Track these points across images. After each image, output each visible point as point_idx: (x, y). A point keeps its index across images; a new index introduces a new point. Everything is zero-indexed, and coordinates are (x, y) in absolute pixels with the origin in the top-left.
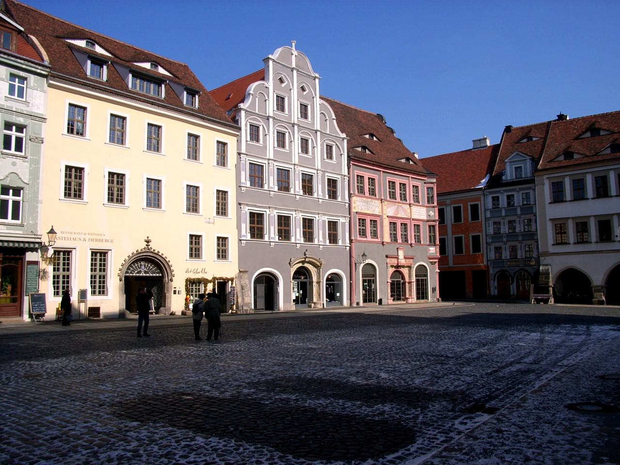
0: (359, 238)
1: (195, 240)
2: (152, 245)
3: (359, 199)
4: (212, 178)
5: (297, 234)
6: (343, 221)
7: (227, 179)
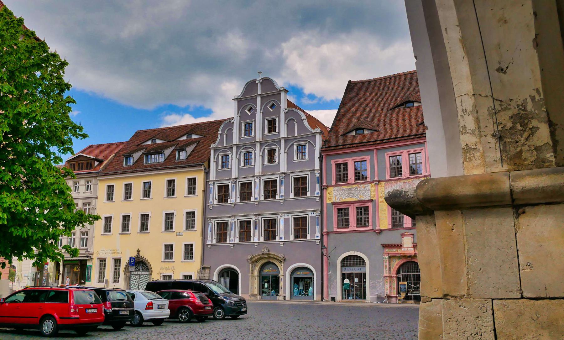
0: (335, 230)
1: (169, 249)
2: (141, 254)
3: (336, 188)
4: (184, 203)
5: (257, 235)
6: (312, 215)
7: (195, 204)
